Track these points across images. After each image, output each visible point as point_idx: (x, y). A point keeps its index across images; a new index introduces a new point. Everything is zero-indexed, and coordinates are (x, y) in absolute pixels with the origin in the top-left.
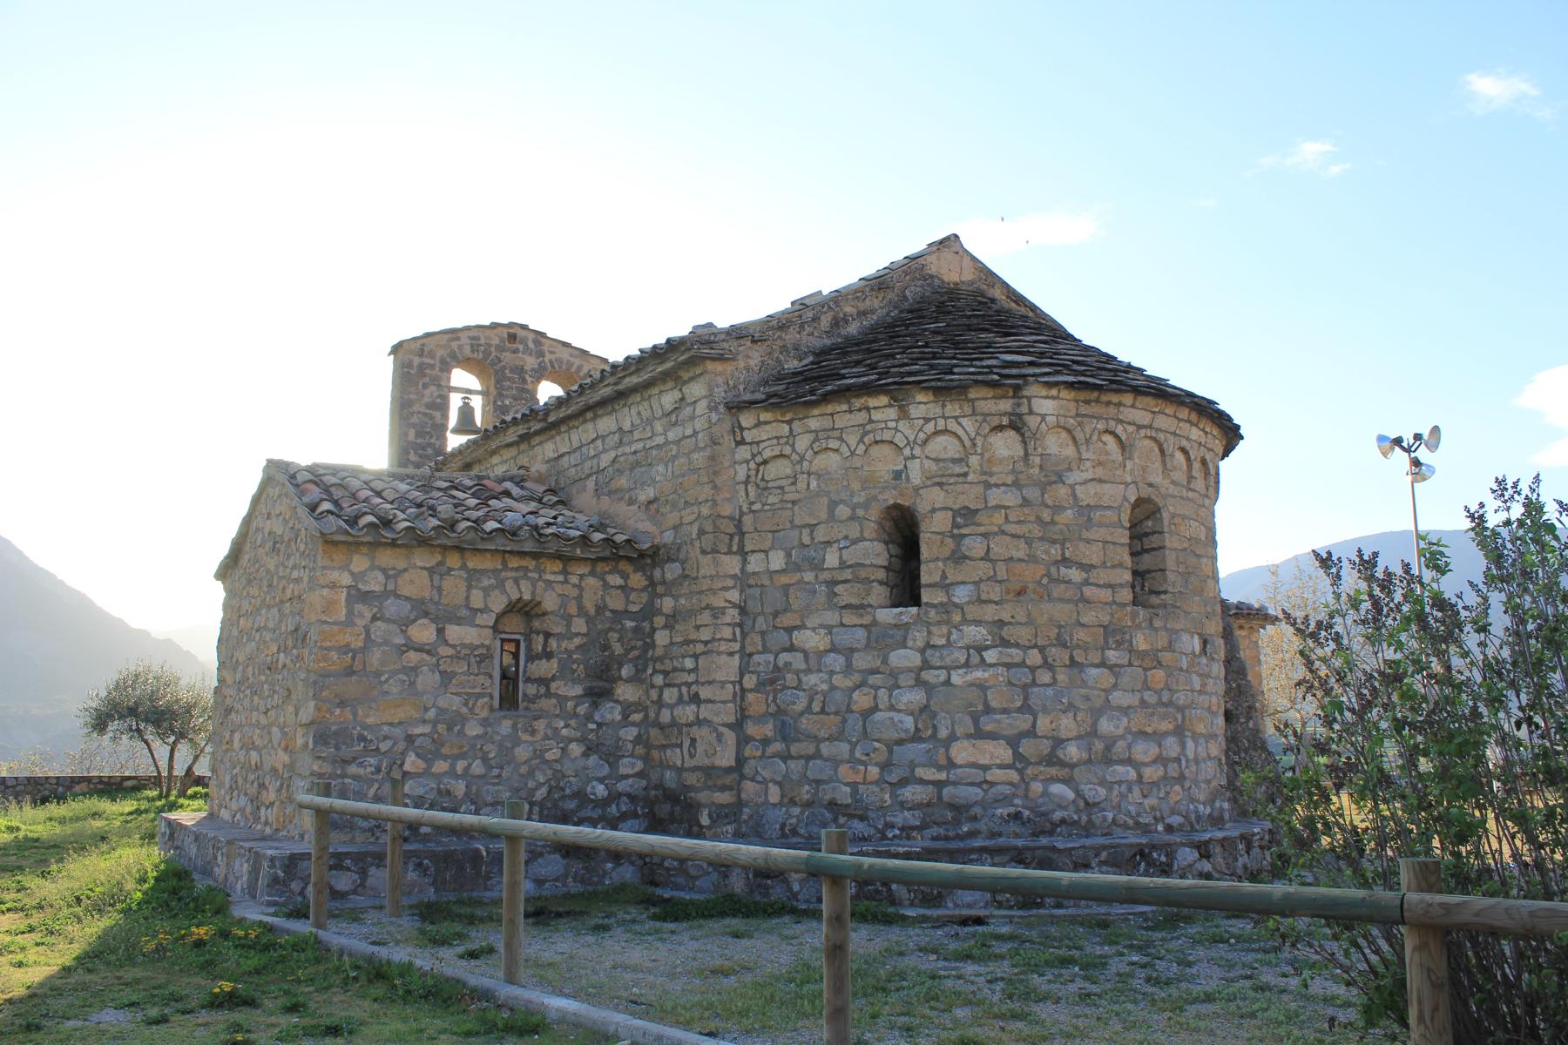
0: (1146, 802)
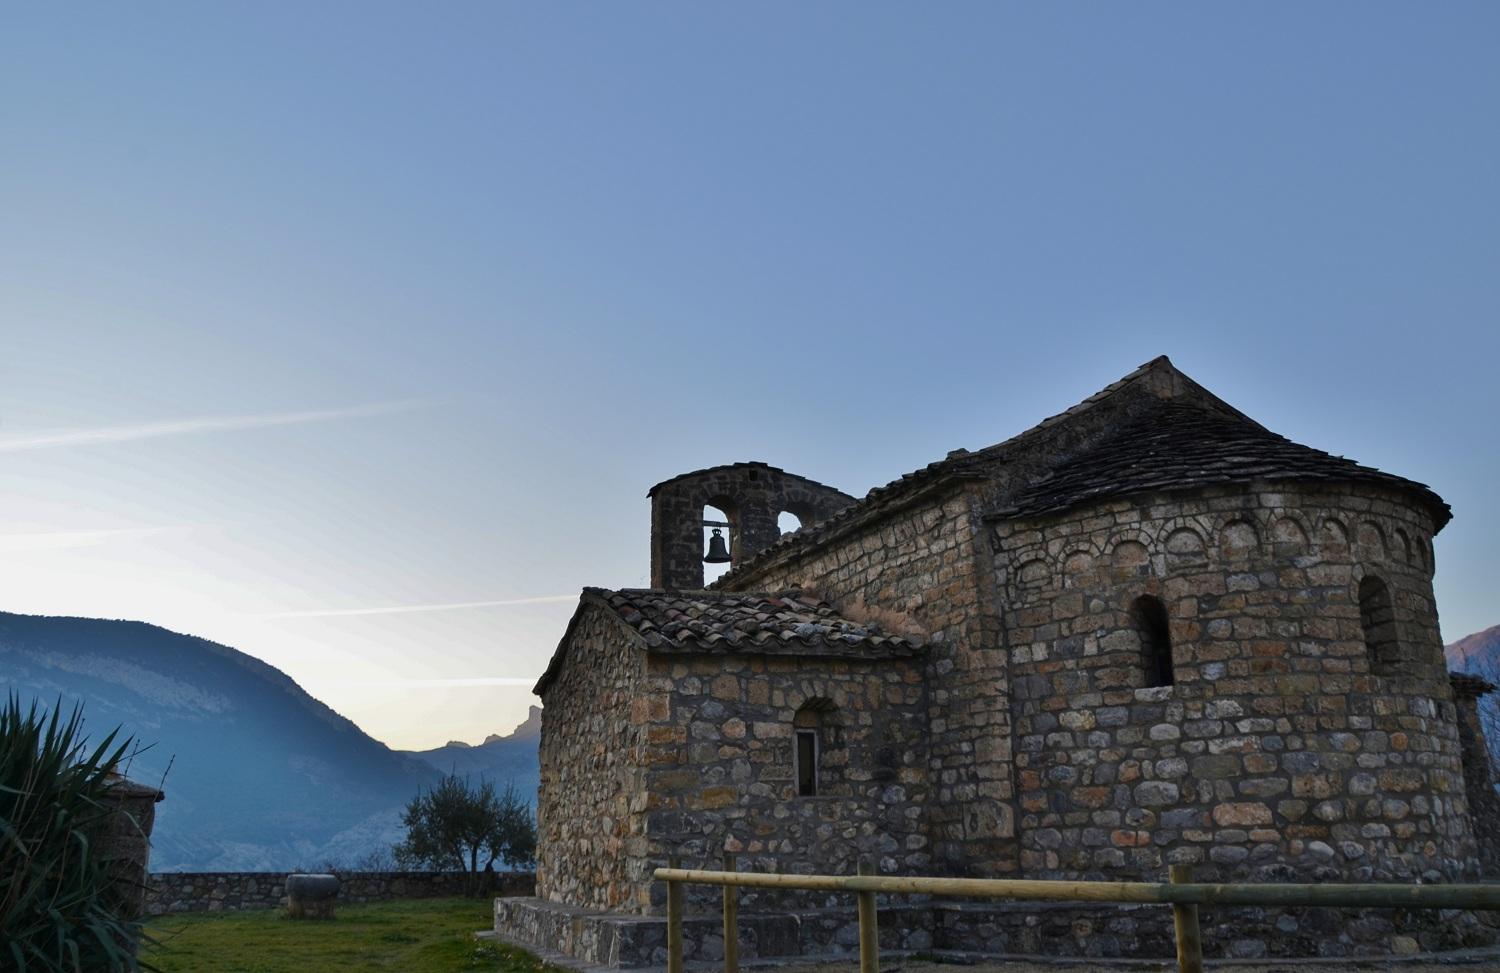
0: (1404, 857)
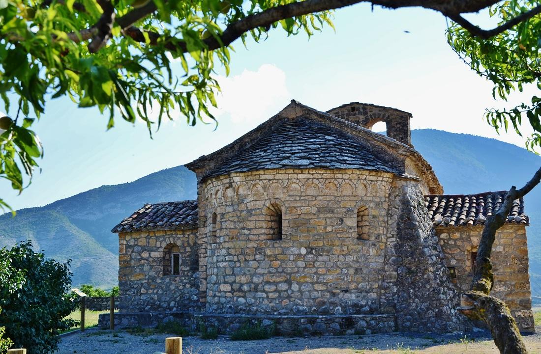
0: (270, 304)
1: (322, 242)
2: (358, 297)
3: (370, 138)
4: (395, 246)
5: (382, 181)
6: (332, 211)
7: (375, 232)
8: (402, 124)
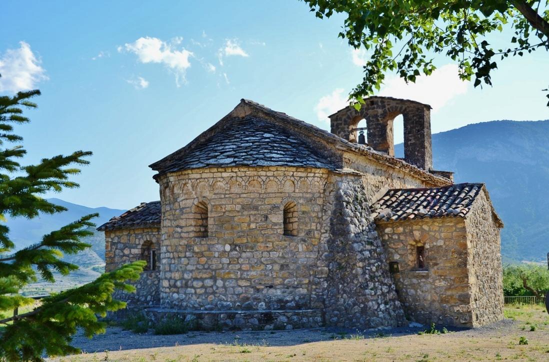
0: (198, 300)
1: (245, 239)
2: (283, 292)
3: (311, 135)
4: (328, 241)
5: (314, 177)
6: (256, 208)
7: (305, 228)
8: (418, 116)
